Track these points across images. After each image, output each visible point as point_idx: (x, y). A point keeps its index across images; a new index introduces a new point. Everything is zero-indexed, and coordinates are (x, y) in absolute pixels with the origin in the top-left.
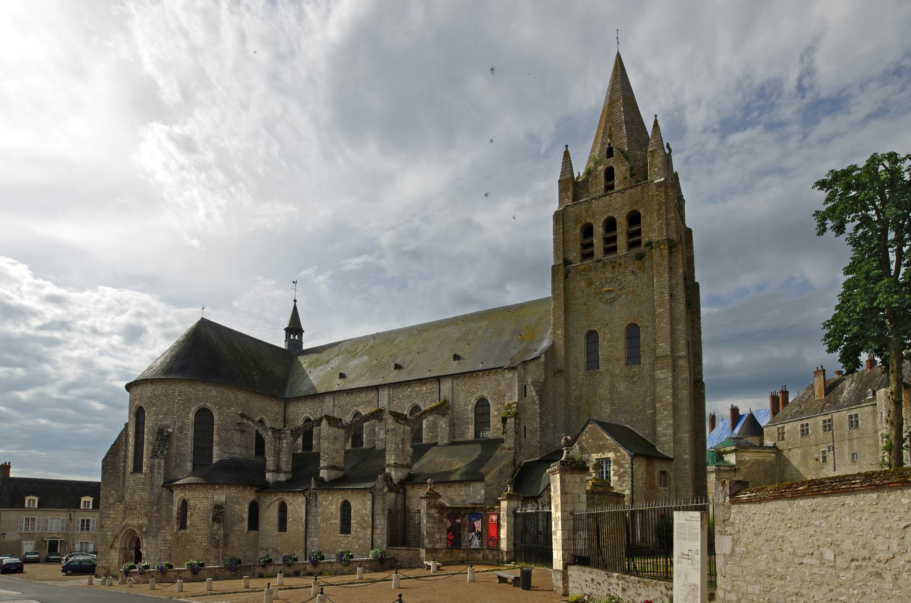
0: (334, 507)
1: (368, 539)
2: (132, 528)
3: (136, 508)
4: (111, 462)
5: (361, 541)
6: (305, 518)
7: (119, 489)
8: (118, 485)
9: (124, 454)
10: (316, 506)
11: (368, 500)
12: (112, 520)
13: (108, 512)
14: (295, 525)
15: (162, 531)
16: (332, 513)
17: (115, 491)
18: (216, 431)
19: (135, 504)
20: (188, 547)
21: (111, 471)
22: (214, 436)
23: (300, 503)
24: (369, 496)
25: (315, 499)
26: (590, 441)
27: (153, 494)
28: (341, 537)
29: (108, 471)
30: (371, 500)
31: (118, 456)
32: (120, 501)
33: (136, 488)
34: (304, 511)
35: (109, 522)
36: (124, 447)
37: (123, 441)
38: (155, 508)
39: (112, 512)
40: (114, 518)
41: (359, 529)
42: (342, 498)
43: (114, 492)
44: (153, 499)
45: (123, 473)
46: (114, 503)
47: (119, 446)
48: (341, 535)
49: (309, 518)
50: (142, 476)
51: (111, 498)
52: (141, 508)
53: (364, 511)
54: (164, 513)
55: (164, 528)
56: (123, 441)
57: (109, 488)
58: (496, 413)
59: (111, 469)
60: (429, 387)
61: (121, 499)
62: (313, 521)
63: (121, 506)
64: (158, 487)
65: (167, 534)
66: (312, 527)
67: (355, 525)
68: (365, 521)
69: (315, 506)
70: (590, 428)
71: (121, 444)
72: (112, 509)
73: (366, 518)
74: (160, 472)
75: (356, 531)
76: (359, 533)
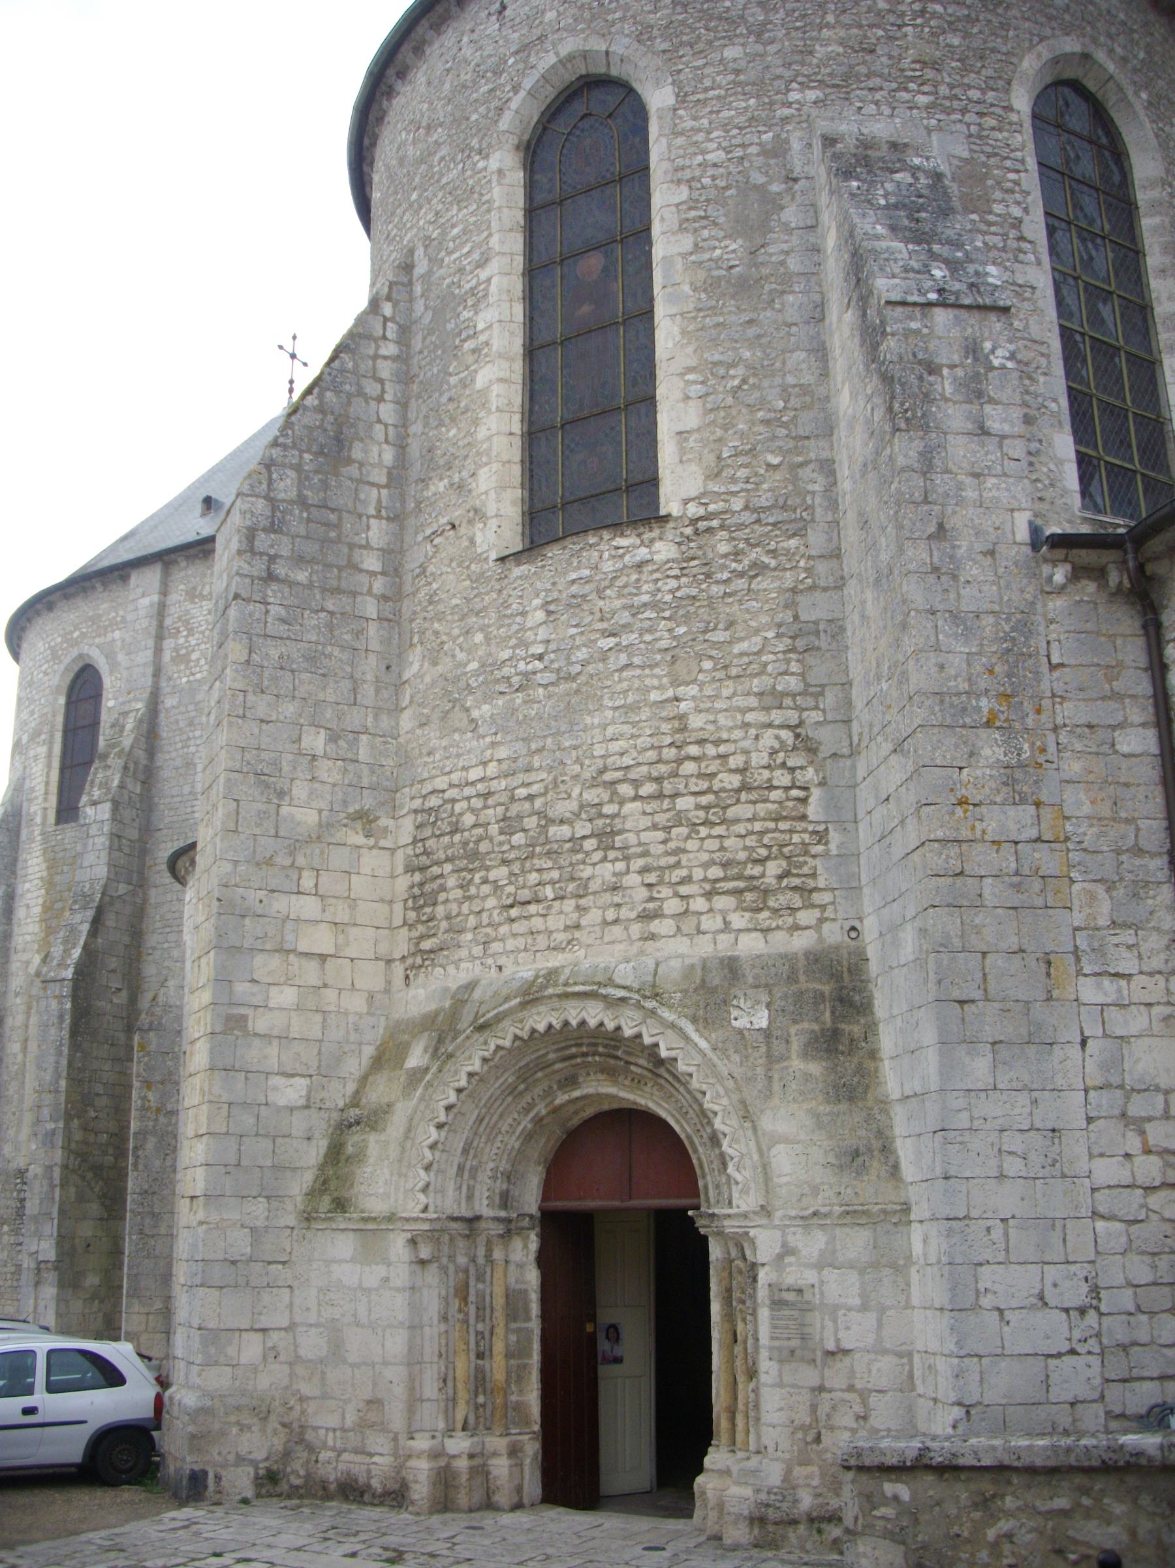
2: (594, 1014)
3: (606, 838)
4: (302, 502)
7: (355, 718)
8: (346, 685)
9: (388, 456)
12: (310, 973)
13: (280, 904)
15: (1089, 991)
17: (333, 738)
18: (1165, 250)
19: (591, 796)
21: (302, 576)
22: (1154, 283)
27: (955, 617)
29: (280, 570)
31: (353, 470)
32: (365, 819)
33: (604, 656)
35: (286, 996)
36: (387, 411)
37: (385, 369)
38: (992, 749)
39: (308, 907)
40: (323, 957)
43: (316, 741)
44: (956, 662)
45: (385, 598)
46: (321, 835)
47: (360, 393)
50: (664, 550)
51: (300, 791)
52: (679, 819)
54: (1078, 802)
55: (1099, 951)
56: (385, 369)
57: (289, 709)
59: (299, 560)
61: (368, 801)
63: (372, 861)
64: (991, 553)
65: (1137, 1021)
71: (372, 388)
72: (308, 882)
74: (995, 425)
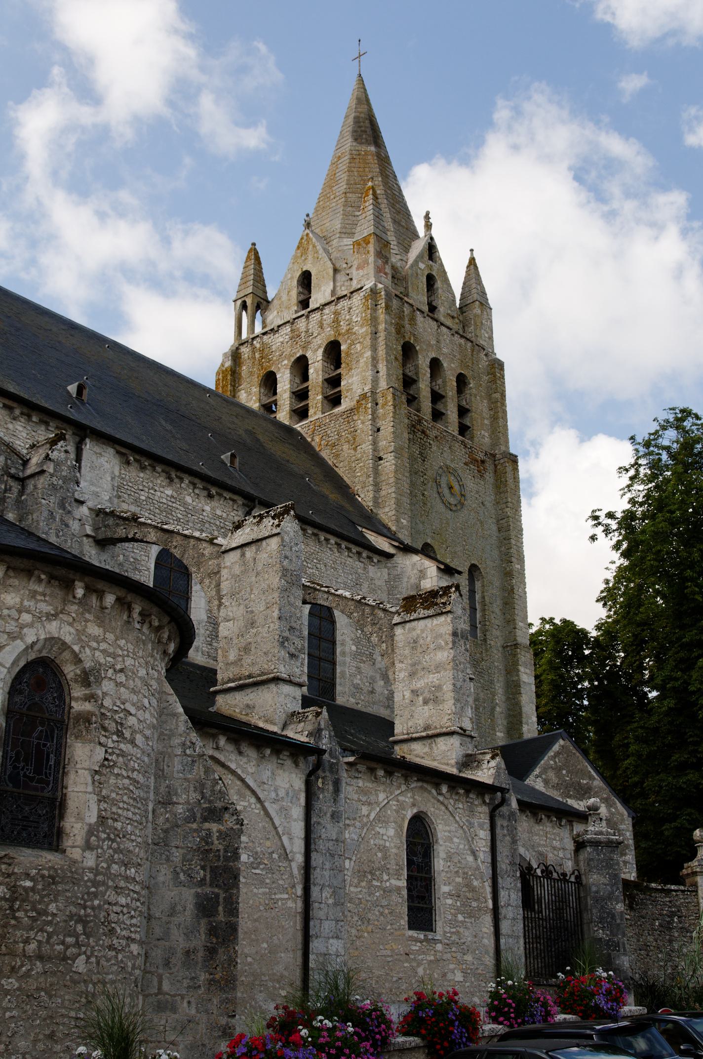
0: (391, 832)
1: (487, 952)
5: (469, 958)
6: (300, 858)
10: (335, 817)
11: (481, 826)
14: (262, 883)
16: (383, 849)
20: (80, 965)
23: (282, 793)
24: (482, 813)
25: (331, 788)
26: (564, 772)
28: (417, 940)
30: (487, 826)
34: (298, 829)
41: (460, 918)
42: (414, 805)
48: (411, 933)
49: (317, 859)
53: (470, 859)
58: (354, 648)
60: (219, 512)
62: (327, 873)
66: (322, 895)
67: (449, 901)
68: (473, 889)
69: (332, 816)
70: (563, 746)
73: (475, 883)
75: (453, 923)
76: (461, 930)
